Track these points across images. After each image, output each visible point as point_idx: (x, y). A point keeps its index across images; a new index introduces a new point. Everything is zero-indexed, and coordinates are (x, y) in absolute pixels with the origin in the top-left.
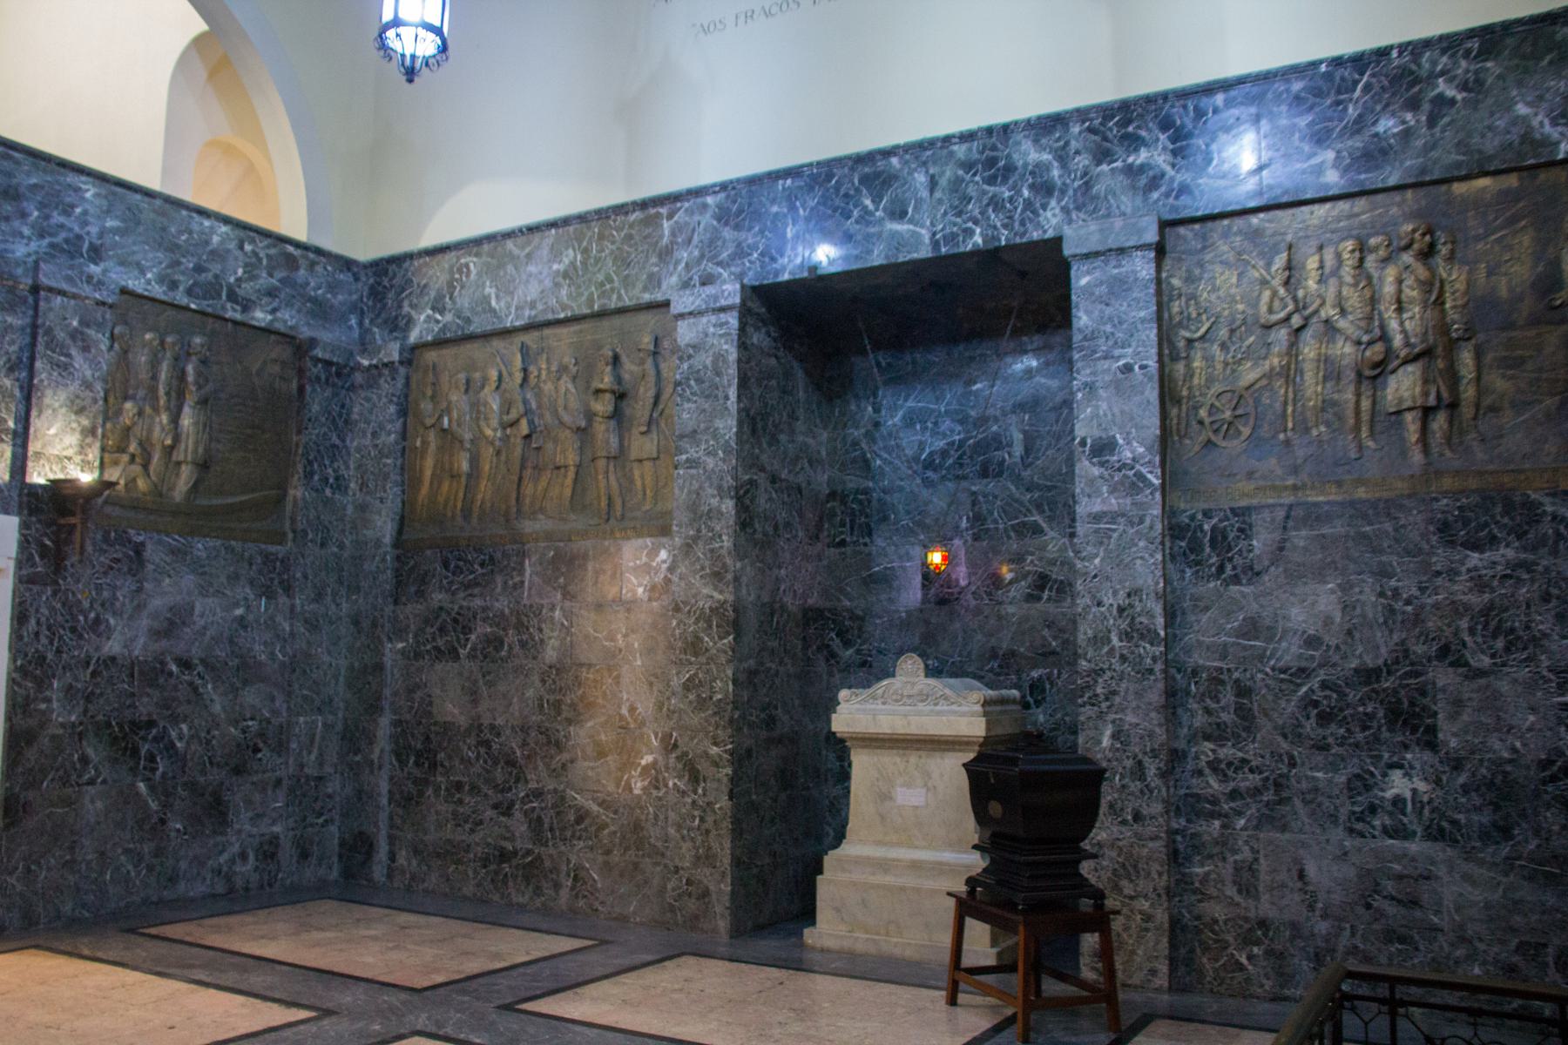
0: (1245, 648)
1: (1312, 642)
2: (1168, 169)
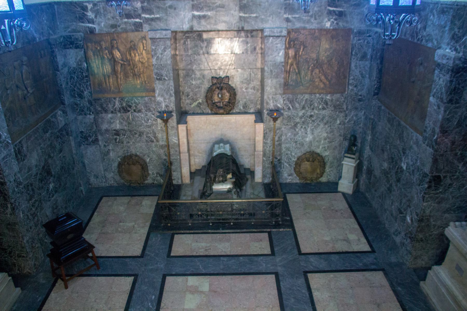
0: (29, 175)
1: (36, 166)
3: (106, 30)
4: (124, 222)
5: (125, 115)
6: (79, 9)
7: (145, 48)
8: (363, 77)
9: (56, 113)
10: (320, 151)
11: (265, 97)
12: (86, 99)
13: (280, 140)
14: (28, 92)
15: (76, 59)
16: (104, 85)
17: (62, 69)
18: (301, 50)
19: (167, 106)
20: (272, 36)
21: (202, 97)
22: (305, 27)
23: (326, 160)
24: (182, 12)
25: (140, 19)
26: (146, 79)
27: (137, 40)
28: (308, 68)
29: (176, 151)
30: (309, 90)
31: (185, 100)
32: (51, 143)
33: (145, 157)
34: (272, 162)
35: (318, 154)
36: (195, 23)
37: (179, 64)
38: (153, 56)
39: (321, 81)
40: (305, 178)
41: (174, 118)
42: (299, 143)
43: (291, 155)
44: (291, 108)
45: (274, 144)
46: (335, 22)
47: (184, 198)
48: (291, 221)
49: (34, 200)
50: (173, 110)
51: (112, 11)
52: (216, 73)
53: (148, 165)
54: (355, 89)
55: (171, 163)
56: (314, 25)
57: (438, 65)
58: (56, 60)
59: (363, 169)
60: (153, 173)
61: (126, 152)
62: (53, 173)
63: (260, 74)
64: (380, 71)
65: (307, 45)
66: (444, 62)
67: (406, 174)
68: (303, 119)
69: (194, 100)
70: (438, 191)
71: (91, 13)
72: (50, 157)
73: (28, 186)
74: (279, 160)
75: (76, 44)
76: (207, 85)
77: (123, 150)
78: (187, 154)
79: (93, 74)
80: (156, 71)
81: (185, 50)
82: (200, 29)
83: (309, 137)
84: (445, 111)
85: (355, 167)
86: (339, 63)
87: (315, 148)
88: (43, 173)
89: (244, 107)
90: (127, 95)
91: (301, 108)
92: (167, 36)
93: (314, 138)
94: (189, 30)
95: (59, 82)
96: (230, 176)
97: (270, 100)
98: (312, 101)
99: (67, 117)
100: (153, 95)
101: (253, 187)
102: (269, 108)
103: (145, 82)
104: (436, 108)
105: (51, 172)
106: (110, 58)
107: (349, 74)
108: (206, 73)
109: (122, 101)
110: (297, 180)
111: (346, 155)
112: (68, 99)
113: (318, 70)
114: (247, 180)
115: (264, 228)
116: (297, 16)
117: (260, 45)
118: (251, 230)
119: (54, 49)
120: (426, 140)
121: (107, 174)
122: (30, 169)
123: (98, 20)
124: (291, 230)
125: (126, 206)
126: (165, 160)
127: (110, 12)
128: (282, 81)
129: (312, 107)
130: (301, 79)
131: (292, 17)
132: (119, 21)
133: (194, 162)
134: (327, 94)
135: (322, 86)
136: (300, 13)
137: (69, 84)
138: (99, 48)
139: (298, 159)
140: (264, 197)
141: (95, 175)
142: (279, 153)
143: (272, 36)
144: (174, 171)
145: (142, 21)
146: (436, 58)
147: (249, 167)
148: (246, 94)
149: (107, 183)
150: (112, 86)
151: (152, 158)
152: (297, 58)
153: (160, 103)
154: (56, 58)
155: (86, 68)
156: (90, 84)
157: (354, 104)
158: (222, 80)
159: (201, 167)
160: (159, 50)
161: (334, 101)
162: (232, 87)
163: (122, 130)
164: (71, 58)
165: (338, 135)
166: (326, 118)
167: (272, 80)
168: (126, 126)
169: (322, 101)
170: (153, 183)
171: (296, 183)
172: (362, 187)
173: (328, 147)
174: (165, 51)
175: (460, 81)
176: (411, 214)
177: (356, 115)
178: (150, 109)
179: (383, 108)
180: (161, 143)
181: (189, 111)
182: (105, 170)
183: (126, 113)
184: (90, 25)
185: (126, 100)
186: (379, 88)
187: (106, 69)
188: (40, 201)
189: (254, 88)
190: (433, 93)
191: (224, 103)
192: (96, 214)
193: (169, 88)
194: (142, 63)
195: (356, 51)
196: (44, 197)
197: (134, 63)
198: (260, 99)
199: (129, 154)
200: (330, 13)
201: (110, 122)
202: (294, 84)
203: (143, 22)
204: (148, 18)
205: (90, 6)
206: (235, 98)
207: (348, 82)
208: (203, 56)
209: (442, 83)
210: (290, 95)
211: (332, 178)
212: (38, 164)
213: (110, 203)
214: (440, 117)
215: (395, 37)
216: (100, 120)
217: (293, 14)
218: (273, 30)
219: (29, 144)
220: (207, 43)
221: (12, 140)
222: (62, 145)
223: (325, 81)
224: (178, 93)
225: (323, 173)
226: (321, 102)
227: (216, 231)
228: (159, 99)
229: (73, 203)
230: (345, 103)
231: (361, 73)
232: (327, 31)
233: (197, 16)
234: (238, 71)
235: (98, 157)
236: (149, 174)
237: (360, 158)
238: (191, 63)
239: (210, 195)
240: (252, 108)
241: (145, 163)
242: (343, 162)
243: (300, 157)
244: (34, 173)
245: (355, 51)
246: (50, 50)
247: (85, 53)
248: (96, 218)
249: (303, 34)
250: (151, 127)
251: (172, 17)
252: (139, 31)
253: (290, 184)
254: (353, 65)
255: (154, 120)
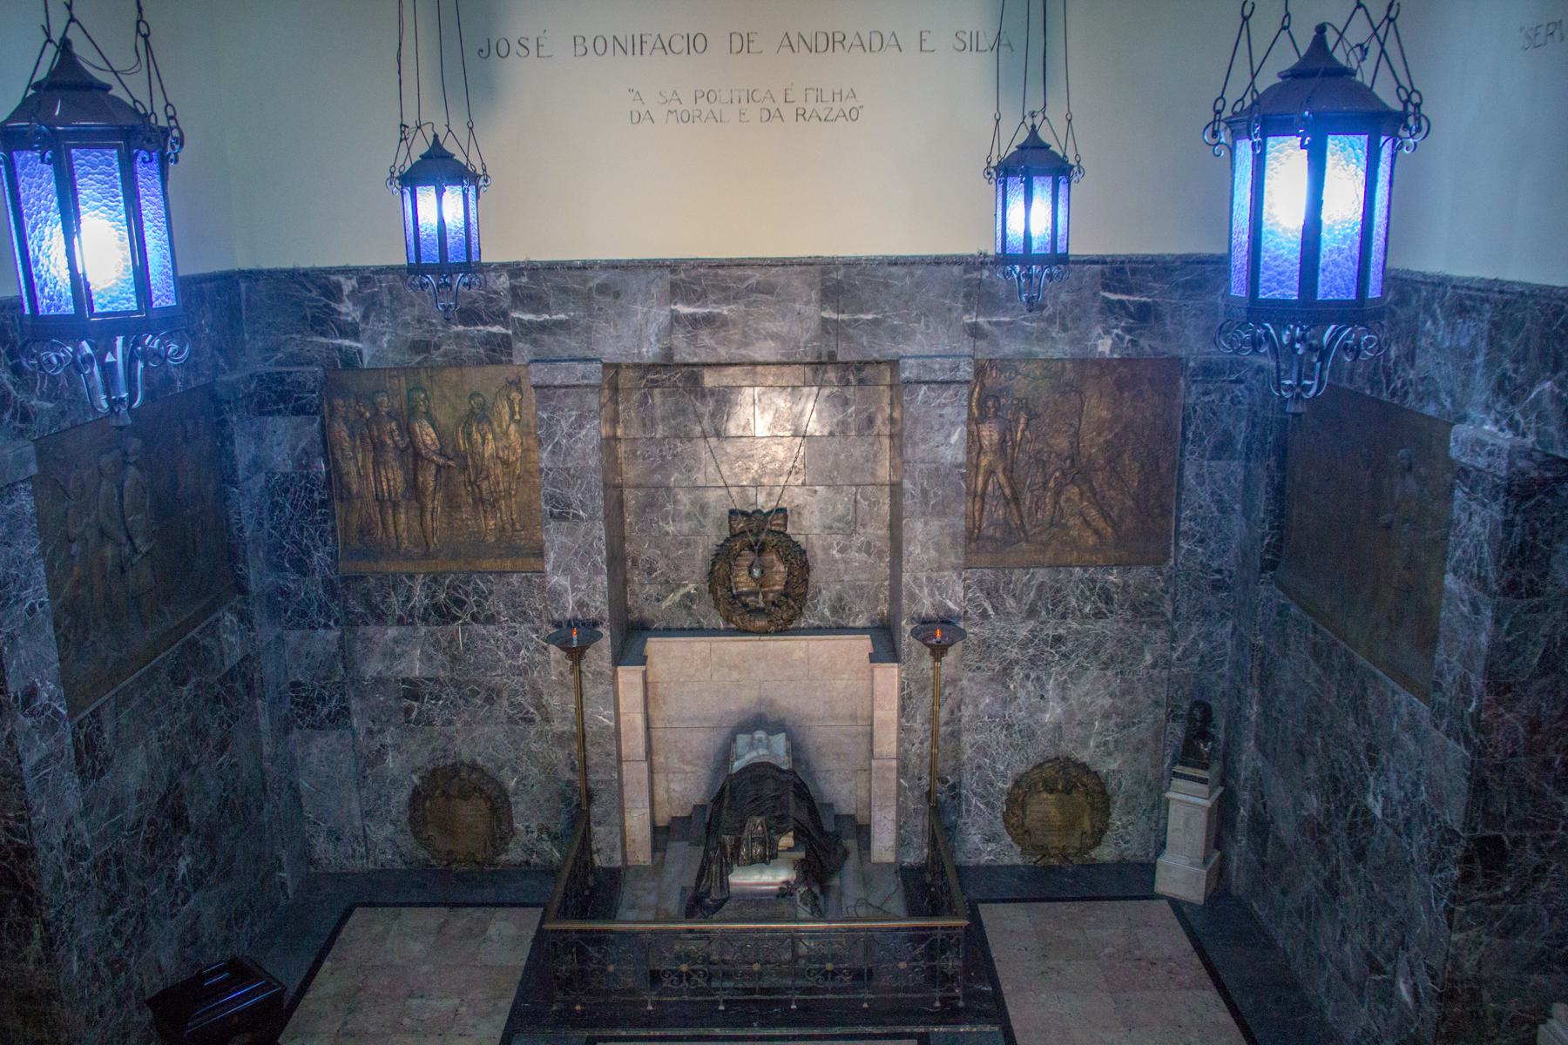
0: (113, 824)
1: (140, 795)
2: (11, 387)
3: (393, 357)
4: (422, 997)
5: (442, 633)
6: (314, 294)
7: (517, 417)
8: (1223, 511)
9: (217, 620)
10: (1092, 757)
11: (906, 578)
12: (318, 577)
13: (954, 719)
14: (135, 551)
15: (294, 448)
16: (379, 533)
17: (248, 478)
18: (1021, 426)
19: (581, 605)
20: (926, 383)
21: (696, 577)
22: (1031, 353)
23: (1112, 785)
24: (639, 307)
25: (505, 325)
26: (514, 516)
27: (494, 390)
28: (1046, 483)
29: (608, 755)
30: (1050, 555)
31: (642, 585)
32: (194, 720)
33: (503, 772)
34: (929, 795)
35: (1084, 765)
36: (679, 339)
37: (624, 467)
38: (540, 442)
39: (1087, 523)
40: (1042, 850)
41: (605, 646)
42: (1020, 731)
43: (994, 769)
44: (991, 612)
45: (934, 734)
46: (1128, 337)
47: (631, 915)
48: (997, 997)
49: (121, 912)
50: (601, 618)
51: (418, 301)
52: (743, 496)
53: (512, 799)
54: (1200, 550)
55: (590, 796)
56: (1059, 348)
57: (1463, 472)
58: (229, 448)
59: (1239, 819)
60: (528, 827)
61: (439, 754)
62: (193, 820)
63: (887, 501)
64: (1279, 492)
65: (1040, 410)
66: (1481, 462)
67: (1383, 831)
68: (1031, 651)
69: (670, 585)
70: (1499, 893)
71: (350, 305)
72: (186, 765)
73: (107, 862)
74: (953, 787)
75: (298, 399)
76: (713, 536)
77: (430, 747)
78: (645, 765)
79: (346, 497)
80: (550, 489)
81: (645, 425)
82: (696, 360)
83: (1054, 709)
84: (1497, 621)
85: (1210, 811)
86: (1143, 466)
87: (1071, 745)
88: (159, 821)
89: (834, 610)
90: (453, 566)
91: (1024, 615)
92: (588, 378)
93: (1069, 714)
94: (659, 361)
95: (233, 521)
96: (786, 841)
97: (921, 588)
98: (1058, 591)
99: (252, 634)
100: (537, 567)
101: (866, 881)
102: (920, 615)
103: (513, 525)
104: (1465, 610)
105: (187, 817)
106: (402, 445)
107: (1178, 504)
108: (712, 496)
109: (434, 587)
110: (1014, 857)
111: (1178, 769)
112: (258, 576)
113: (1076, 490)
114: (846, 854)
115: (906, 1024)
116: (1007, 319)
117: (888, 411)
118: (860, 1029)
119: (228, 417)
120: (1442, 717)
121: (372, 828)
122: (117, 805)
123: (373, 325)
124: (996, 1028)
125: (432, 939)
126: (569, 783)
127: (413, 305)
128: (961, 525)
129: (1060, 609)
130: (1021, 517)
131: (989, 323)
132: (437, 331)
133: (668, 791)
134: (1107, 567)
135: (1091, 540)
136: (1013, 308)
137: (267, 525)
138: (368, 414)
139: (1017, 784)
140: (903, 914)
141: (330, 832)
142: (951, 763)
143: (926, 383)
144: (599, 823)
145: (510, 332)
146: (1454, 452)
147: (853, 812)
148: (841, 567)
149: (372, 858)
150: (405, 535)
151: (526, 778)
152: (1009, 451)
153: (560, 595)
154: (232, 443)
155: (323, 477)
156: (334, 530)
157: (1197, 599)
158: (765, 521)
159: (690, 808)
160: (563, 423)
161: (1131, 589)
162: (796, 544)
163: (430, 680)
164: (279, 444)
165: (1149, 701)
166: (1108, 645)
167: (926, 524)
168: (443, 666)
169: (1090, 590)
170: (527, 863)
171: (1014, 867)
172: (1239, 882)
173: (1116, 741)
174: (581, 427)
175: (1538, 525)
176: (1412, 974)
177: (1208, 636)
178: (525, 613)
179: (1294, 610)
180: (558, 726)
181: (653, 622)
182: (367, 815)
183: (446, 623)
184: (347, 343)
185: (447, 582)
186: (1277, 547)
187: (388, 480)
188: (142, 915)
189: (867, 548)
190: (1453, 562)
191: (771, 596)
192: (327, 964)
193: (591, 545)
194: (506, 463)
195: (1197, 427)
196: (156, 904)
197: (479, 463)
198: (887, 583)
199: (449, 761)
200: (1109, 308)
201: (393, 653)
202: (998, 535)
203: (514, 333)
204: (530, 322)
205: (348, 285)
206: (806, 580)
207: (1177, 526)
208: (701, 443)
209: (1480, 530)
210: (986, 571)
211: (1134, 850)
212: (146, 788)
213: (378, 928)
214: (1483, 639)
215: (1311, 393)
216: (358, 646)
217: (991, 315)
218: (928, 361)
219: (124, 721)
220: (717, 401)
221: (69, 708)
222: (229, 726)
223: (1101, 524)
224: (618, 562)
225: (1102, 832)
226: (1088, 593)
227: (739, 1032)
228: (558, 580)
229: (252, 925)
230: (1168, 597)
231: (1216, 497)
232: (1104, 364)
233: (686, 316)
234: (816, 492)
235: (345, 771)
236: (513, 831)
237: (1227, 777)
238: (662, 467)
239: (718, 906)
240: (862, 612)
241: (504, 792)
242: (1169, 795)
243: (1023, 776)
244: (133, 817)
245: (1193, 427)
246: (215, 419)
247: (324, 429)
248: (328, 982)
249: (1026, 376)
250: (526, 673)
251: (607, 321)
252: (500, 362)
253: (991, 870)
254: (1189, 473)
255: (536, 650)
